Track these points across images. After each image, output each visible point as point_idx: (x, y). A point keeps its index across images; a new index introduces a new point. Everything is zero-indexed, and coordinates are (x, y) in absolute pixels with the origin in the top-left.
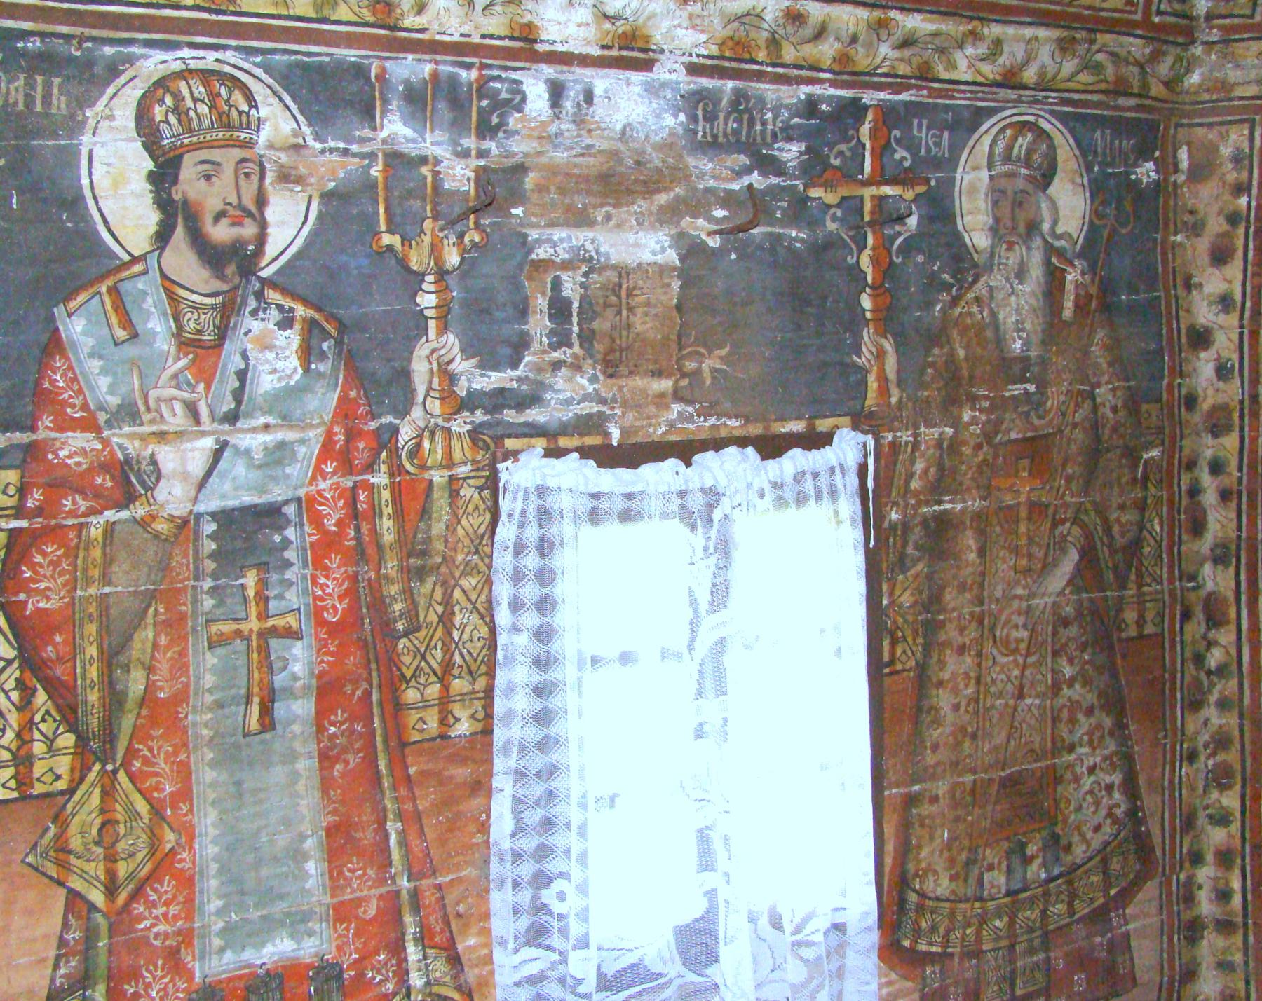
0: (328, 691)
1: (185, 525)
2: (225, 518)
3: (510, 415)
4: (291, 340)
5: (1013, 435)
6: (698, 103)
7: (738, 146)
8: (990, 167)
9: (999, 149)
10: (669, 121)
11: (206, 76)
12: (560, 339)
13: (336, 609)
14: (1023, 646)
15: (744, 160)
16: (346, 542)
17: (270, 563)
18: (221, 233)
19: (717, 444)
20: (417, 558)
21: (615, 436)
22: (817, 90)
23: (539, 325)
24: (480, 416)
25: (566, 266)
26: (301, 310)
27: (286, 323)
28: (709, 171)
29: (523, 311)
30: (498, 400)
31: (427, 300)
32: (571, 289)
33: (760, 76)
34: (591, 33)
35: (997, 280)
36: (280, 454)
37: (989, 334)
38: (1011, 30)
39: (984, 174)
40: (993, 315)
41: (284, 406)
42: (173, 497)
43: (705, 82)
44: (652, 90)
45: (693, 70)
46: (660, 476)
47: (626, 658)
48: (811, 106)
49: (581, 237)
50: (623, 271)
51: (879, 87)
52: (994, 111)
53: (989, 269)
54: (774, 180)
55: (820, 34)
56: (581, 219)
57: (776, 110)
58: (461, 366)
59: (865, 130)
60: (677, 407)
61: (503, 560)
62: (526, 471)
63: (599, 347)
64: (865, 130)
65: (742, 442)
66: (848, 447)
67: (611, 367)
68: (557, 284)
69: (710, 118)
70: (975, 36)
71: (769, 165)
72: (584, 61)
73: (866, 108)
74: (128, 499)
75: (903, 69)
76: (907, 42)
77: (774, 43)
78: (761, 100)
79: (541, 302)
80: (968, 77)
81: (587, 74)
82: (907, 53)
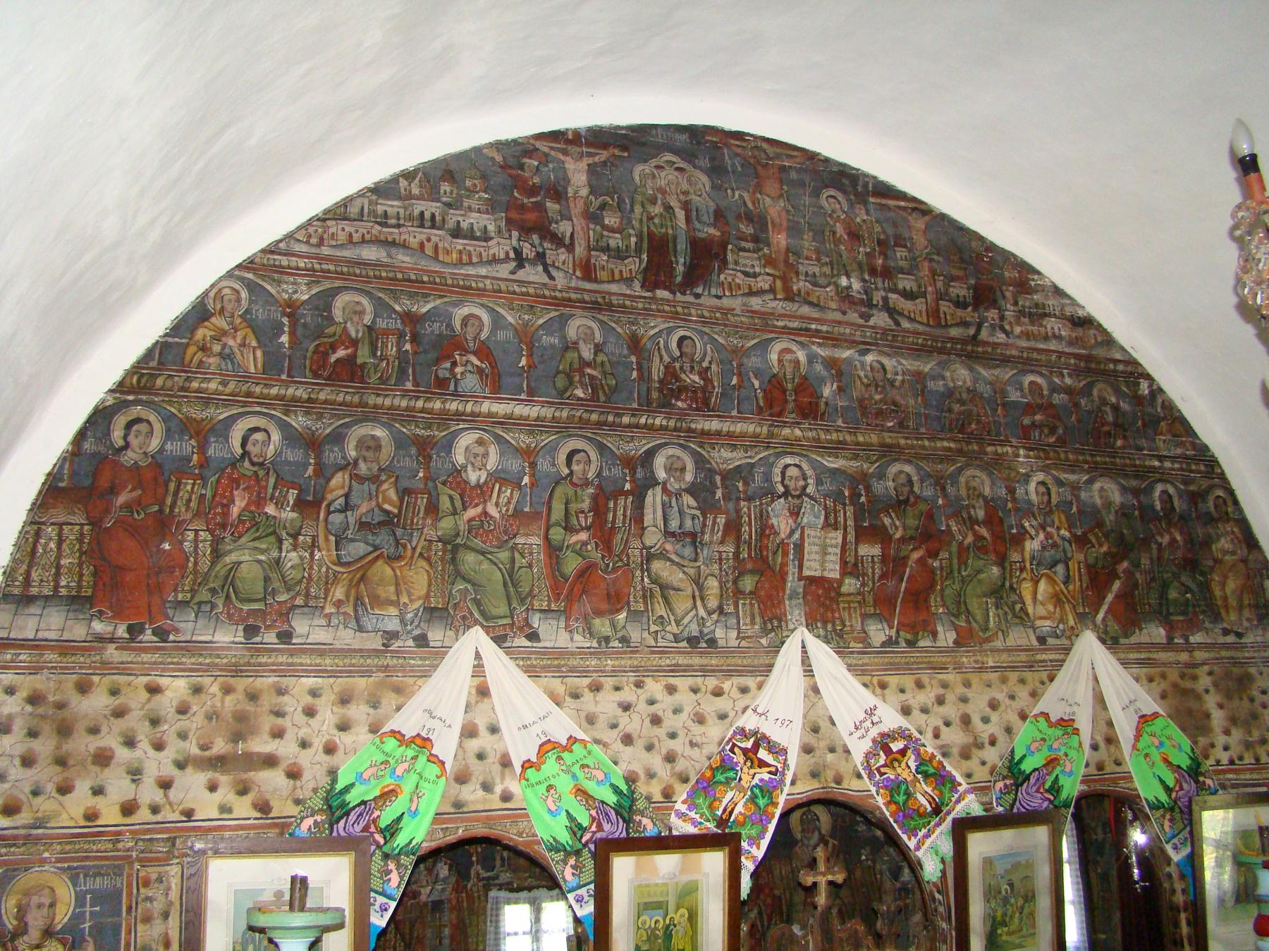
0: (452, 938)
1: (425, 904)
2: (433, 902)
4: (446, 867)
12: (503, 865)
13: (455, 922)
16: (457, 908)
17: (442, 911)
19: (538, 887)
20: (471, 911)
23: (498, 863)
30: (488, 879)
31: (474, 859)
36: (443, 890)
41: (445, 880)
42: (423, 898)
46: (524, 894)
61: (489, 913)
62: (493, 893)
67: (514, 871)
74: (415, 898)
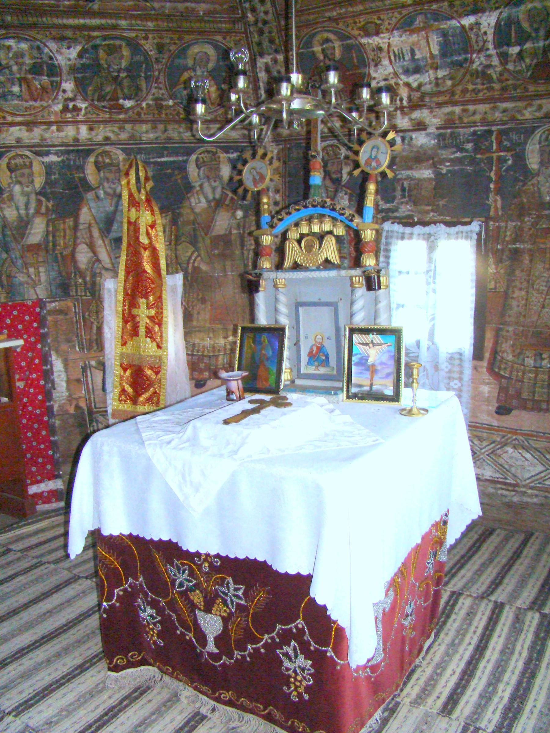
3: (391, 214)
4: (346, 197)
5: (544, 226)
6: (440, 137)
7: (453, 147)
8: (540, 143)
9: (544, 137)
10: (433, 142)
11: (332, 146)
12: (403, 196)
14: (545, 292)
15: (455, 150)
18: (334, 176)
19: (435, 223)
21: (416, 220)
22: (477, 128)
23: (398, 193)
24: (384, 214)
25: (405, 179)
26: (349, 191)
27: (346, 194)
28: (444, 154)
29: (394, 190)
32: (406, 184)
33: (457, 127)
34: (410, 124)
35: (541, 178)
37: (537, 195)
38: (544, 101)
39: (538, 146)
40: (539, 189)
43: (442, 131)
44: (428, 135)
45: (438, 128)
46: (418, 229)
47: (408, 273)
48: (474, 133)
49: (409, 173)
50: (419, 180)
51: (497, 125)
52: (538, 127)
53: (538, 175)
54: (464, 154)
55: (474, 113)
56: (411, 168)
57: (464, 135)
58: (381, 203)
59: (493, 138)
60: (432, 214)
63: (413, 198)
64: (493, 138)
65: (440, 222)
66: (475, 226)
67: (415, 204)
68: (403, 184)
69: (444, 140)
70: (531, 105)
71: (461, 150)
72: (409, 131)
73: (493, 131)
75: (504, 119)
76: (505, 111)
77: (460, 118)
78: (459, 133)
79: (399, 188)
80: (530, 117)
81: (410, 133)
82: (505, 114)
